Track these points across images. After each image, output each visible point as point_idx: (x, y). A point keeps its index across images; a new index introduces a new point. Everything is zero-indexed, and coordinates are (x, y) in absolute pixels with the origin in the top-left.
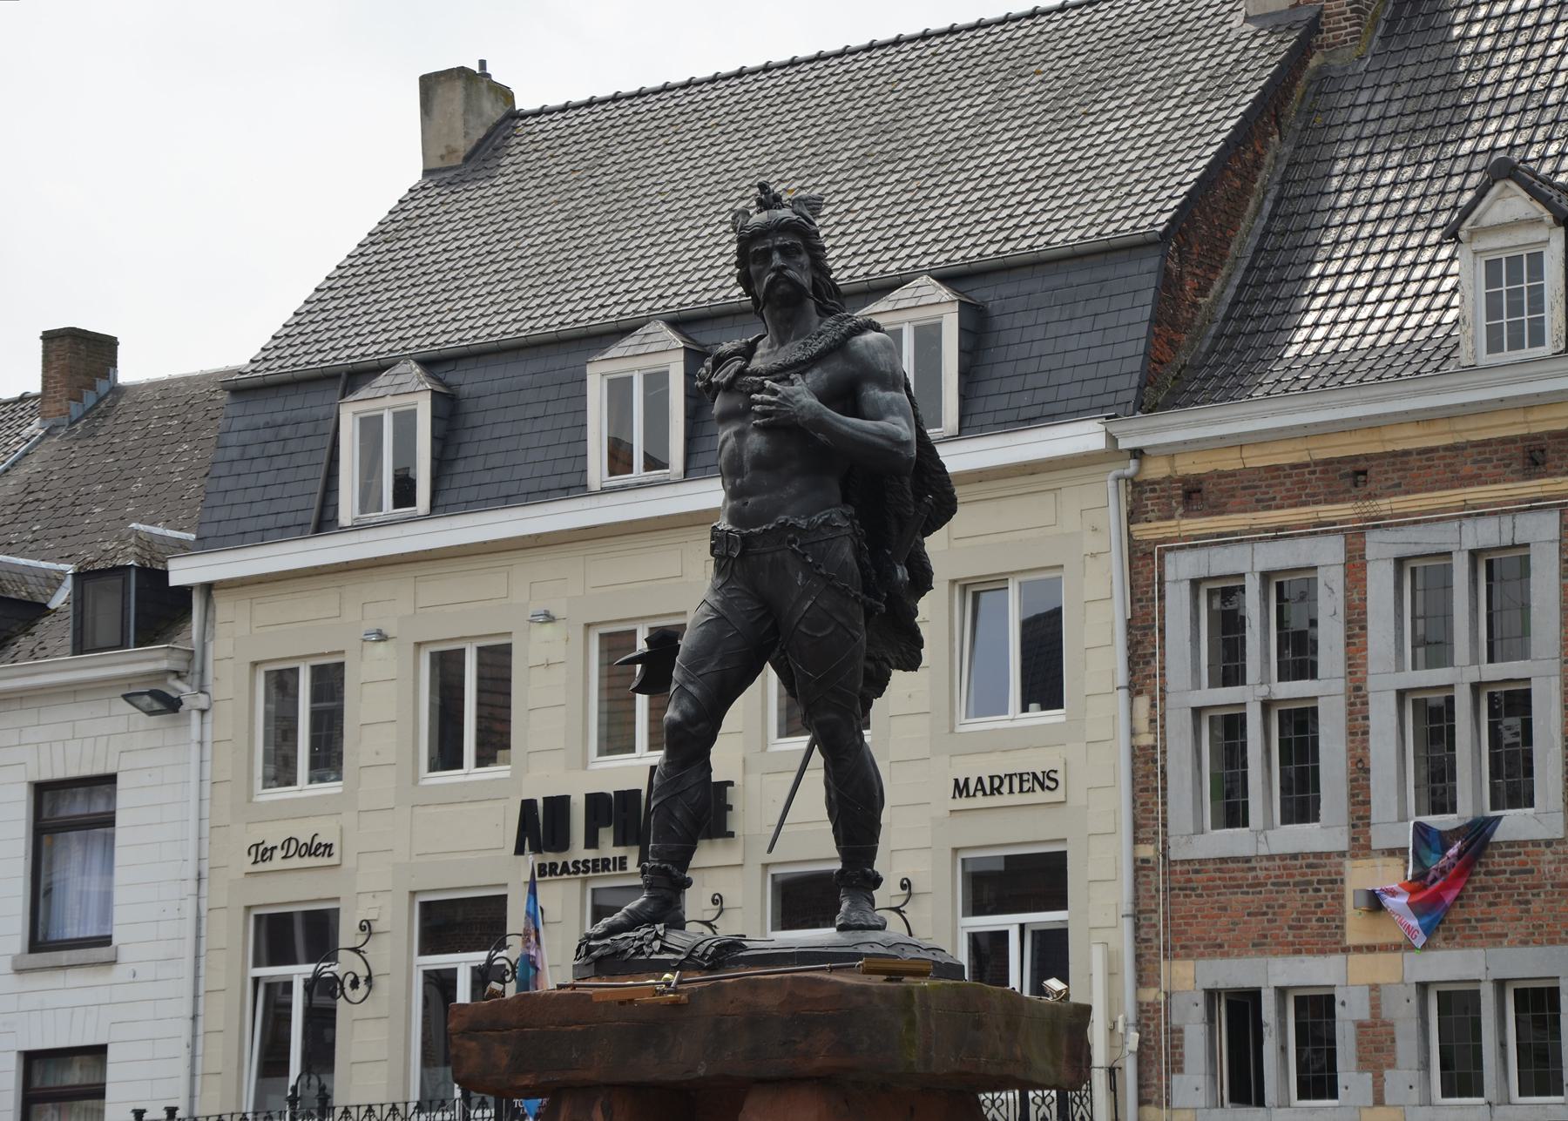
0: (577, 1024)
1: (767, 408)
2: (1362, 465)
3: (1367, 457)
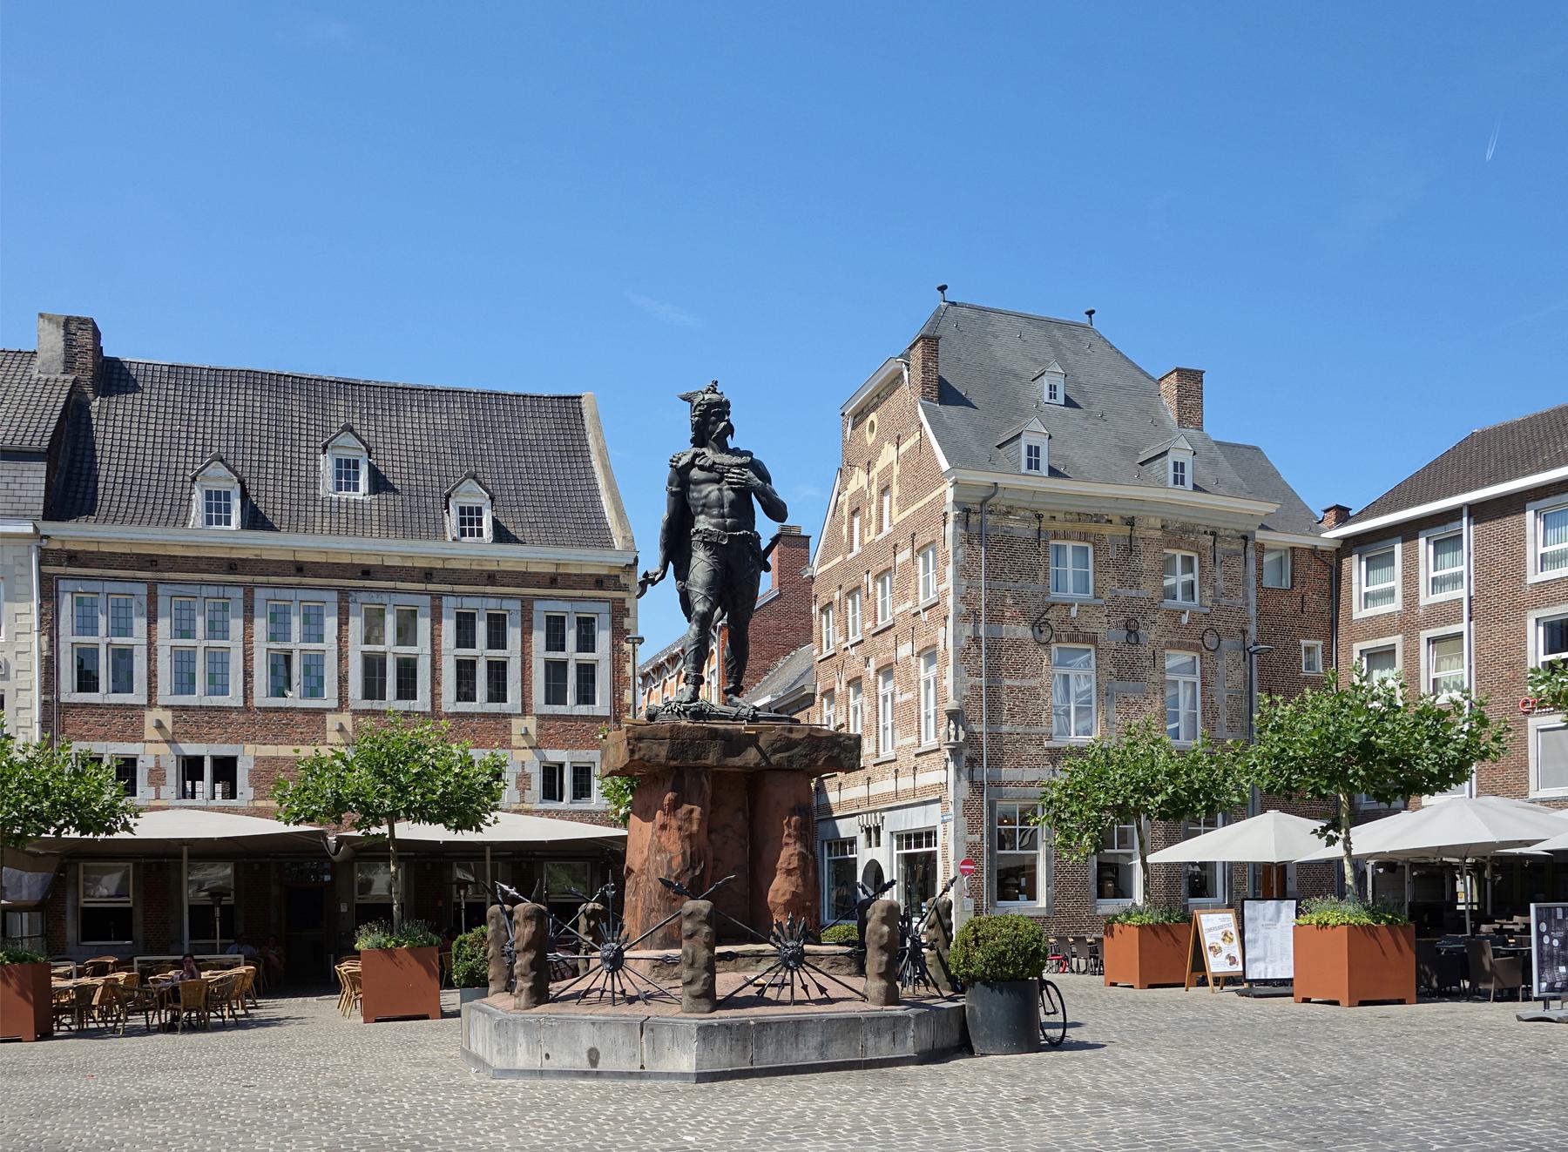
2: (155, 558)
3: (157, 555)
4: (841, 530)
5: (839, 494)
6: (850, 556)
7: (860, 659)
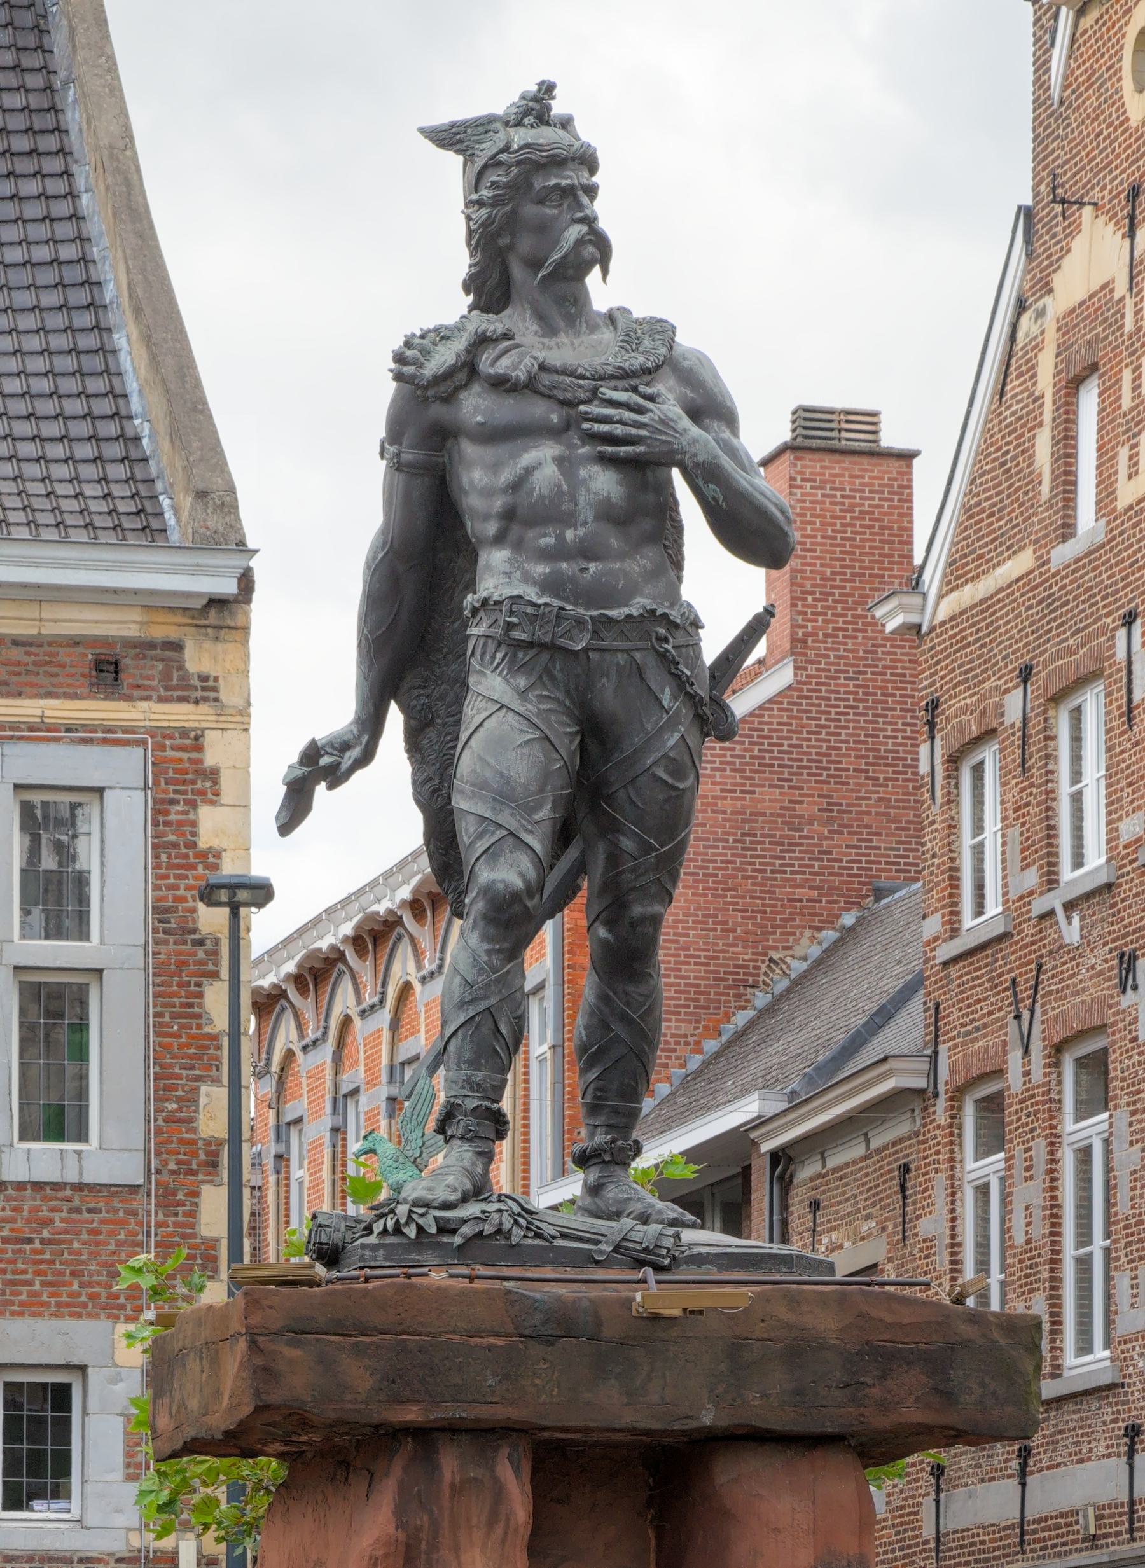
0: (497, 1335)
1: (634, 431)
4: (1028, 452)
5: (1021, 306)
6: (1063, 554)
7: (1101, 958)
